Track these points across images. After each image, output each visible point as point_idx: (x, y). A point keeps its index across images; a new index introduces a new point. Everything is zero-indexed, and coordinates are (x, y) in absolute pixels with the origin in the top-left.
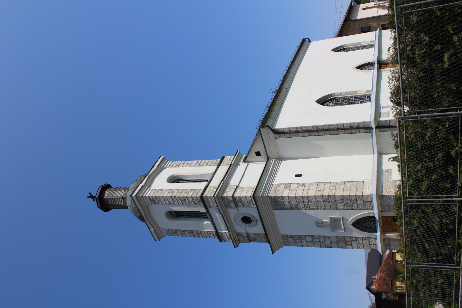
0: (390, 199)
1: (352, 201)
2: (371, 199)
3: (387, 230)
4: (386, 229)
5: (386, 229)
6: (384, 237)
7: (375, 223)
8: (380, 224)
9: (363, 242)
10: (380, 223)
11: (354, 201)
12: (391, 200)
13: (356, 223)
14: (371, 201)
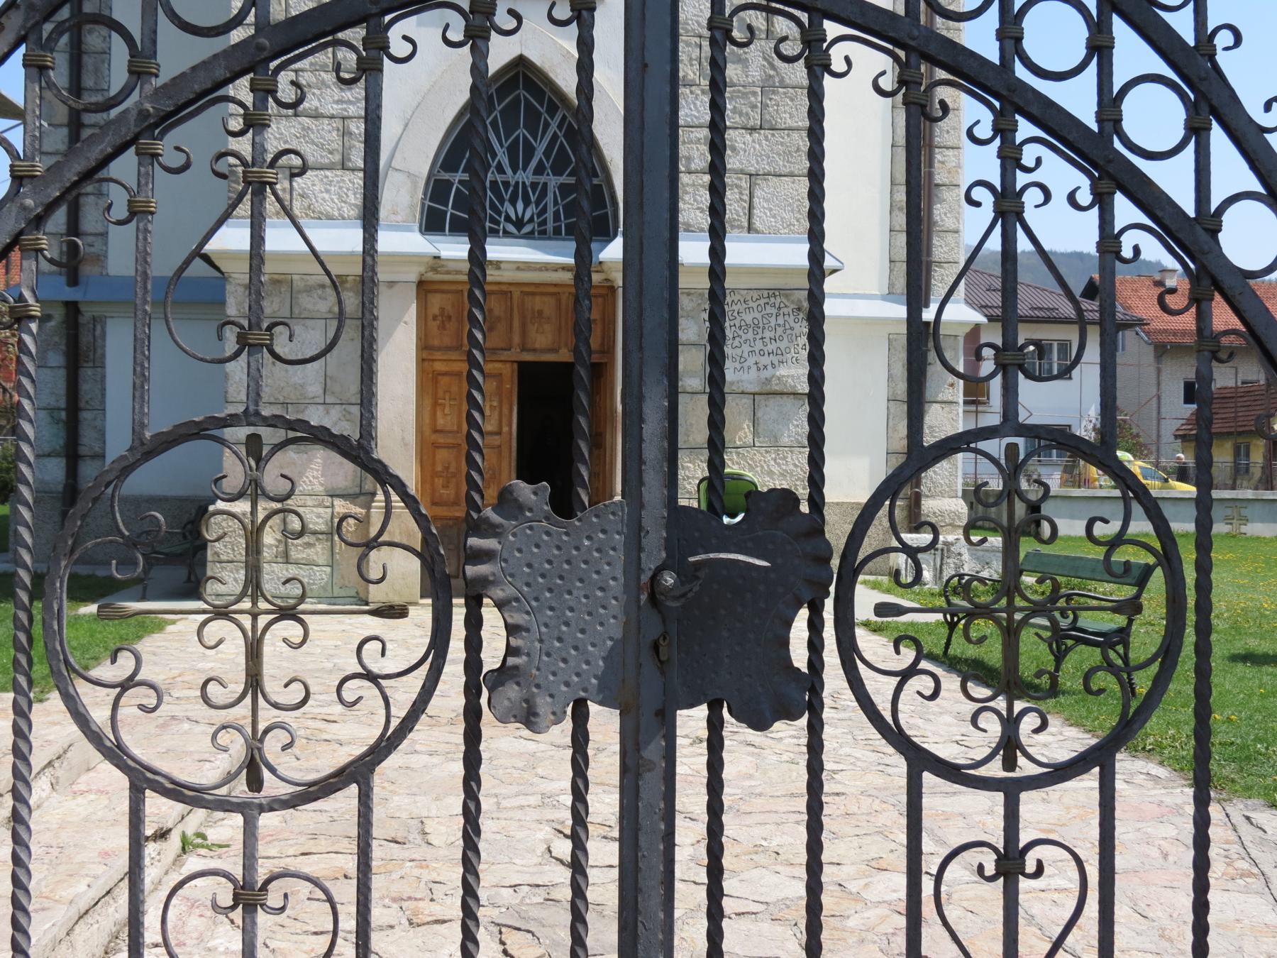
0: (775, 359)
1: (754, 94)
2: (777, 232)
3: (434, 310)
4: (436, 302)
5: (442, 309)
6: (391, 284)
7: (519, 231)
8: (518, 269)
9: (316, 116)
10: (545, 267)
11: (753, 107)
12: (765, 360)
13: (523, 93)
14: (757, 223)
